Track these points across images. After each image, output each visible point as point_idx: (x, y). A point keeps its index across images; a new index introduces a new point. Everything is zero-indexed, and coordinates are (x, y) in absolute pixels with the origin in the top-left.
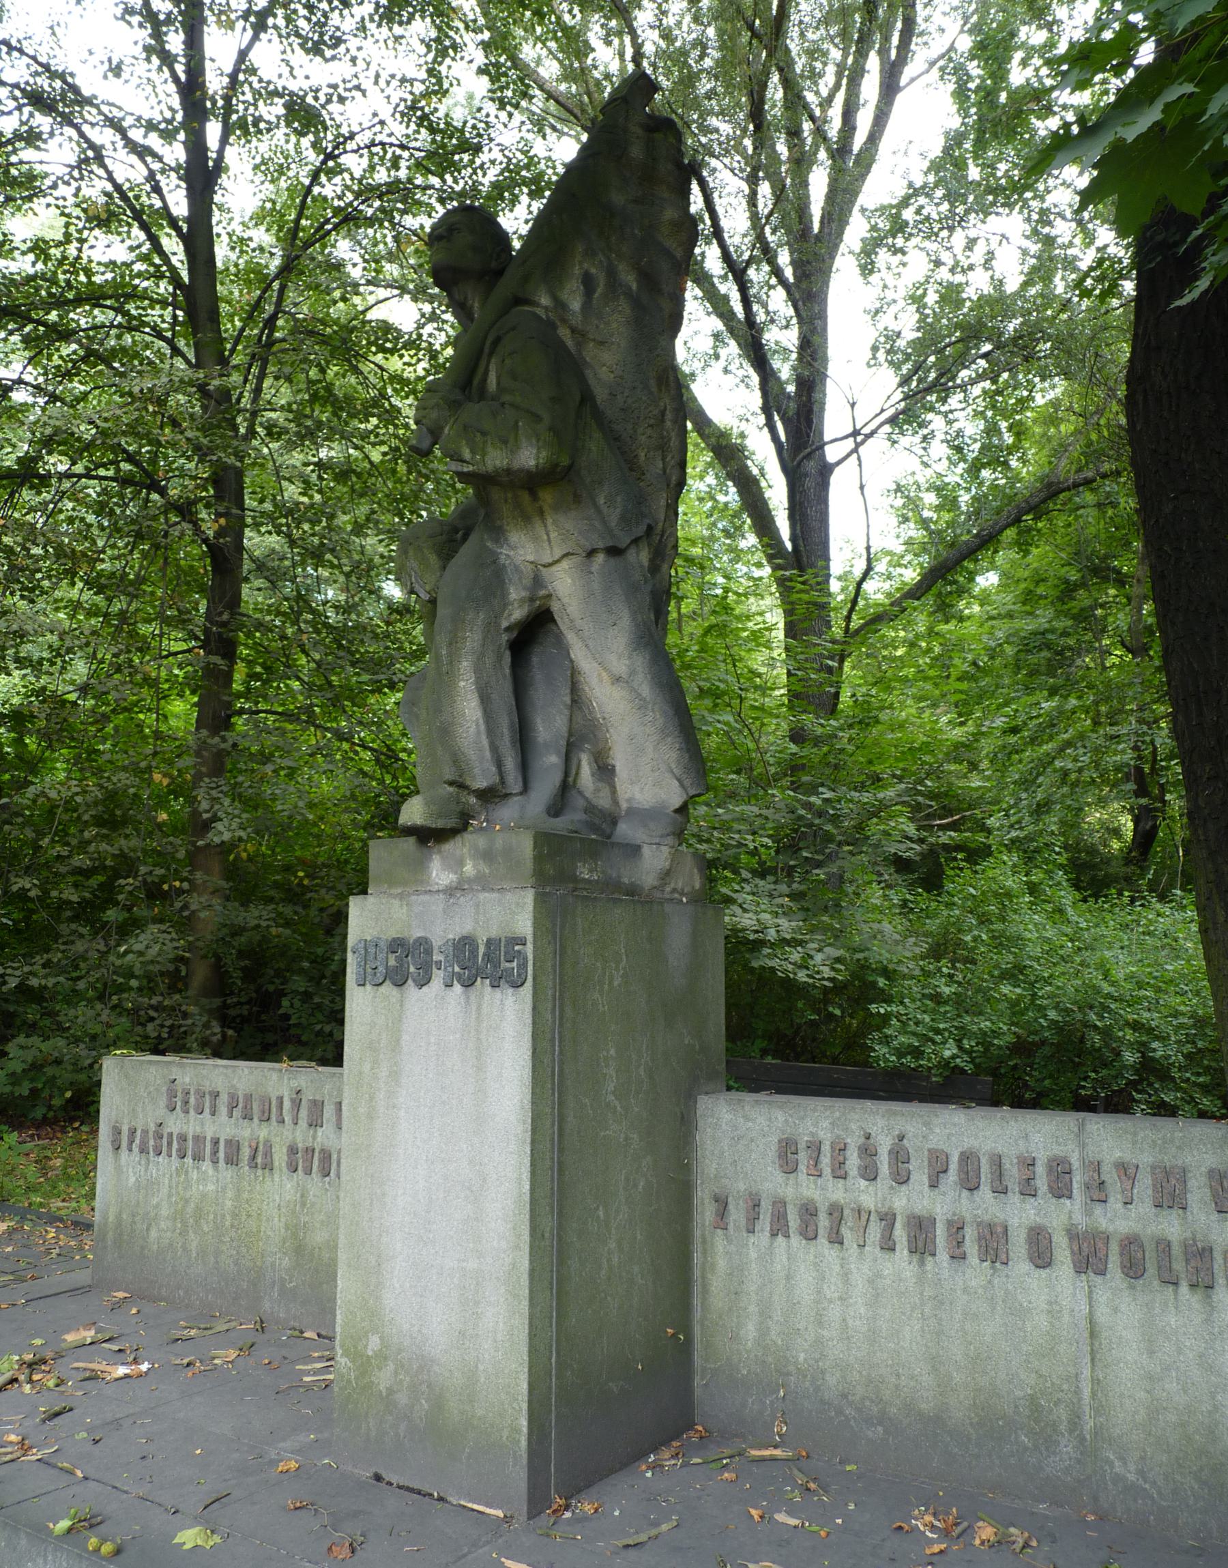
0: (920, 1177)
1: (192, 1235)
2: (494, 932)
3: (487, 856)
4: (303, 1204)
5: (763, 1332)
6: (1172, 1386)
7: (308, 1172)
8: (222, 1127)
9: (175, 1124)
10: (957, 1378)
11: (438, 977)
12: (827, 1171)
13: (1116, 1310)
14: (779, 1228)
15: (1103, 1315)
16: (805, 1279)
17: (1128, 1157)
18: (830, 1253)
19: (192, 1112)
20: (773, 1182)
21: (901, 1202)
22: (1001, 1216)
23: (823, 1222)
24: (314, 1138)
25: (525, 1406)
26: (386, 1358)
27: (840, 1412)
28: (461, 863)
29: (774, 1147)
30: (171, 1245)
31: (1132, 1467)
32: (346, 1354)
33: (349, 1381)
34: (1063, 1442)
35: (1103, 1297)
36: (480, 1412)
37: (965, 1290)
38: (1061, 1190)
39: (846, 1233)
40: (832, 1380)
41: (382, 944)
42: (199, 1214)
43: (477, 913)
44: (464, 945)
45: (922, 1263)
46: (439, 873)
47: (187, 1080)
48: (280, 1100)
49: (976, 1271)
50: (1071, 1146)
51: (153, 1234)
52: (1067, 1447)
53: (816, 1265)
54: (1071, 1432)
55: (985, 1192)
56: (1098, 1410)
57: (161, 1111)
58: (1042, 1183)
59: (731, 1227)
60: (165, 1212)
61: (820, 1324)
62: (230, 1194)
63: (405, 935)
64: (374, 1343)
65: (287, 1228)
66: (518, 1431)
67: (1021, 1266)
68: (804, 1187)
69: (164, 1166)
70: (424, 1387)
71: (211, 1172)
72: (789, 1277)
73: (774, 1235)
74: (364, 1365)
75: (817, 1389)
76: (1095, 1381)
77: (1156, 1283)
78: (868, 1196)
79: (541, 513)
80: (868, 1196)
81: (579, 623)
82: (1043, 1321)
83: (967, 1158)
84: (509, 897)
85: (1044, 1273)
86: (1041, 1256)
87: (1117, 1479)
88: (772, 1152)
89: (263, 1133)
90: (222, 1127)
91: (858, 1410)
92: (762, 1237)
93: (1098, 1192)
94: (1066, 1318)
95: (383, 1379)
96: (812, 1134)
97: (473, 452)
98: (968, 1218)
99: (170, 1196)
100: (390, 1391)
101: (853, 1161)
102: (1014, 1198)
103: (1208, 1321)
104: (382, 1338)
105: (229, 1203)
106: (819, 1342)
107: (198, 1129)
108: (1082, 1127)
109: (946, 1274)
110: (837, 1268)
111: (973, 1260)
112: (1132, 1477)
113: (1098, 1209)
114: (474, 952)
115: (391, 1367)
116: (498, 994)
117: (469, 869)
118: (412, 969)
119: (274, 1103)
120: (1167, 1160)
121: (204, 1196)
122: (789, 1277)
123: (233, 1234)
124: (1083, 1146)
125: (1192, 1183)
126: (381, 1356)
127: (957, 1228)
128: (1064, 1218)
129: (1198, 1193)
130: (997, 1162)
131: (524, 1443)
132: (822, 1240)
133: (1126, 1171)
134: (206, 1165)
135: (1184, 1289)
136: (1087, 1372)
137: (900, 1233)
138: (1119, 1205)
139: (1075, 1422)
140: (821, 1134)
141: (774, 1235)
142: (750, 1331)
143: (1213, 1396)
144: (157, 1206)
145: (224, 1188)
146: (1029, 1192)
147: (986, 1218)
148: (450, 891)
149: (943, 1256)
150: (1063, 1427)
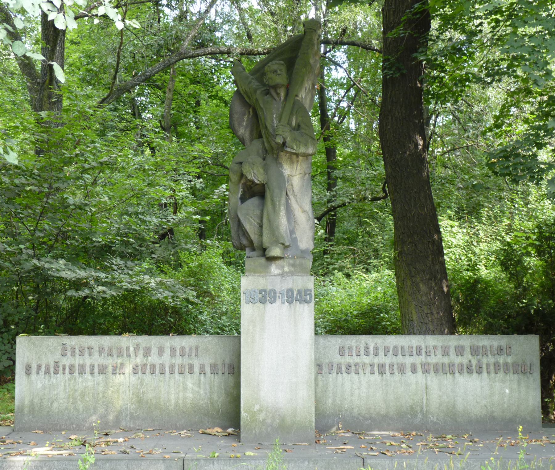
0: (381, 353)
1: (79, 403)
2: (300, 287)
3: (293, 265)
4: (142, 385)
5: (334, 400)
6: (445, 397)
7: (144, 373)
8: (97, 360)
9: (67, 361)
10: (391, 404)
11: (278, 302)
12: (354, 354)
13: (432, 381)
14: (339, 371)
15: (429, 383)
16: (347, 384)
17: (436, 344)
18: (355, 377)
19: (77, 356)
20: (337, 359)
21: (376, 361)
22: (404, 361)
23: (353, 368)
24: (147, 361)
25: (314, 415)
26: (262, 411)
27: (358, 418)
28: (283, 267)
29: (338, 349)
30: (67, 408)
31: (435, 418)
32: (246, 412)
33: (247, 420)
34: (419, 415)
35: (429, 378)
36: (298, 419)
37: (394, 381)
38: (419, 354)
39: (361, 371)
40: (355, 411)
41: (256, 291)
42: (83, 395)
43: (293, 282)
44: (290, 291)
45: (382, 376)
46: (274, 269)
47: (73, 343)
48: (128, 348)
49: (397, 376)
50: (422, 342)
51: (55, 405)
52: (420, 416)
53: (351, 380)
54: (421, 412)
55: (400, 356)
56: (428, 406)
57: (57, 356)
58: (415, 353)
59: (323, 373)
60: (62, 395)
61: (352, 395)
62: (101, 385)
63: (265, 288)
64: (257, 407)
65: (133, 394)
66: (312, 422)
67: (409, 374)
68: (348, 359)
69: (61, 379)
70: (277, 416)
71: (90, 377)
72: (342, 385)
73: (337, 373)
74: (253, 414)
75: (351, 414)
76: (427, 399)
77: (442, 374)
78: (367, 360)
79: (298, 161)
80: (367, 360)
81: (296, 193)
82: (414, 387)
83: (395, 348)
84: (305, 277)
85: (414, 375)
86: (414, 370)
87: (432, 421)
88: (337, 351)
89: (120, 360)
90: (97, 360)
91: (363, 417)
92: (334, 375)
93: (428, 354)
94: (420, 385)
95: (261, 417)
96: (350, 345)
97: (297, 147)
98: (395, 363)
99: (65, 389)
100: (264, 420)
101: (362, 351)
102: (408, 357)
103: (454, 381)
104: (260, 405)
105: (101, 389)
106: (351, 401)
107: (81, 362)
108: (425, 338)
109: (389, 378)
110: (357, 380)
111: (396, 373)
112: (435, 420)
113: (428, 357)
114: (293, 294)
115: (264, 413)
116: (302, 305)
117: (286, 269)
118: (268, 298)
119: (125, 349)
120: (445, 344)
121: (86, 387)
122: (342, 385)
123: (104, 400)
124: (425, 342)
125: (451, 349)
126: (260, 411)
127: (391, 366)
128: (420, 360)
129: (452, 351)
130: (402, 348)
131: (314, 424)
132: (353, 373)
133: (435, 347)
134: (88, 376)
135: (448, 374)
136: (425, 397)
137: (376, 369)
138: (434, 356)
139: (422, 410)
140: (353, 344)
141: (337, 373)
142: (330, 401)
143: (454, 398)
144: (57, 394)
145: (98, 384)
146: (411, 355)
147: (400, 362)
148: (282, 275)
149: (388, 373)
150: (419, 412)
